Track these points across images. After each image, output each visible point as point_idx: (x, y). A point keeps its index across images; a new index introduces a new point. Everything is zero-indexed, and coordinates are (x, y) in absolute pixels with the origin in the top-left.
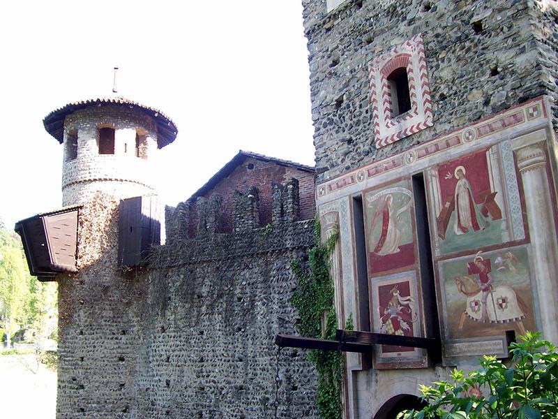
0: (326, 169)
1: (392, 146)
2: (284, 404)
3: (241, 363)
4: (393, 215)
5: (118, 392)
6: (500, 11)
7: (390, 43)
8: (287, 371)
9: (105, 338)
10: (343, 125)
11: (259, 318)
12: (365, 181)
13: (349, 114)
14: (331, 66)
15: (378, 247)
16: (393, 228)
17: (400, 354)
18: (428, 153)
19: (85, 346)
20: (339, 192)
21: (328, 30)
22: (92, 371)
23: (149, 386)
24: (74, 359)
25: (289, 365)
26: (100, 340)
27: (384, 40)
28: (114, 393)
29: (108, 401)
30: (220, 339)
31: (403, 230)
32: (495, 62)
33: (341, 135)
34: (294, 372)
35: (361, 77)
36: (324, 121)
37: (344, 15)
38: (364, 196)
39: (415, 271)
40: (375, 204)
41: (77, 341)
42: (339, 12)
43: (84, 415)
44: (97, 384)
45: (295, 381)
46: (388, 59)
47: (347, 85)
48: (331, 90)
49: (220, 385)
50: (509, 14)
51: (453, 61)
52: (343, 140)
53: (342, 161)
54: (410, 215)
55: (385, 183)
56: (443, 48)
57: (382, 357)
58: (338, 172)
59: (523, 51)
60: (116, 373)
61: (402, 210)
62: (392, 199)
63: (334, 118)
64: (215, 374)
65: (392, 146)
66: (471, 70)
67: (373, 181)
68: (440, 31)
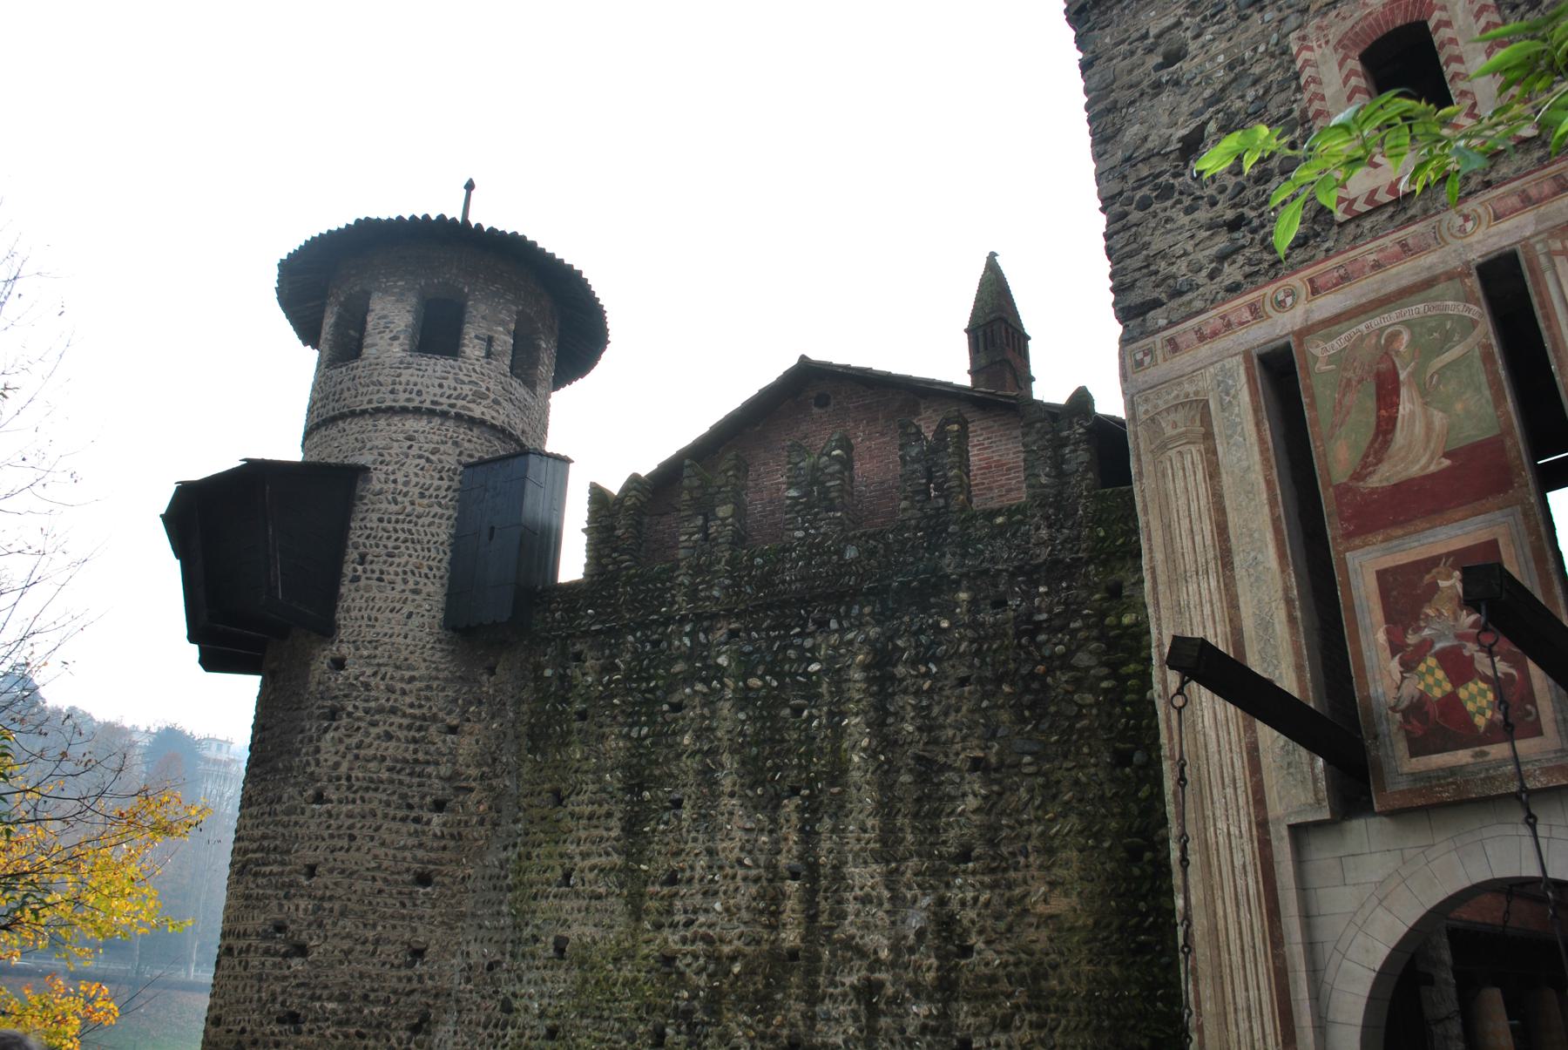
0: (1157, 304)
1: (1391, 209)
2: (930, 999)
3: (796, 885)
4: (1411, 374)
5: (404, 972)
8: (942, 902)
9: (385, 816)
11: (856, 759)
12: (1300, 310)
15: (1365, 466)
16: (1418, 410)
17: (1484, 754)
18: (1527, 201)
19: (326, 834)
20: (1205, 350)
22: (337, 906)
23: (498, 957)
24: (288, 868)
25: (948, 886)
26: (369, 821)
28: (394, 972)
29: (372, 996)
30: (736, 818)
31: (1459, 407)
33: (1203, 215)
34: (963, 903)
35: (1267, 72)
36: (1139, 195)
38: (1301, 344)
39: (1519, 508)
40: (1339, 359)
41: (302, 819)
43: (299, 1032)
44: (346, 944)
45: (967, 931)
48: (1165, 119)
49: (726, 949)
52: (1212, 226)
53: (1212, 276)
54: (1478, 364)
55: (1371, 302)
57: (1406, 769)
58: (1198, 304)
60: (403, 917)
61: (1447, 357)
62: (1405, 337)
63: (1176, 182)
64: (712, 917)
65: (1391, 209)
67: (1329, 304)
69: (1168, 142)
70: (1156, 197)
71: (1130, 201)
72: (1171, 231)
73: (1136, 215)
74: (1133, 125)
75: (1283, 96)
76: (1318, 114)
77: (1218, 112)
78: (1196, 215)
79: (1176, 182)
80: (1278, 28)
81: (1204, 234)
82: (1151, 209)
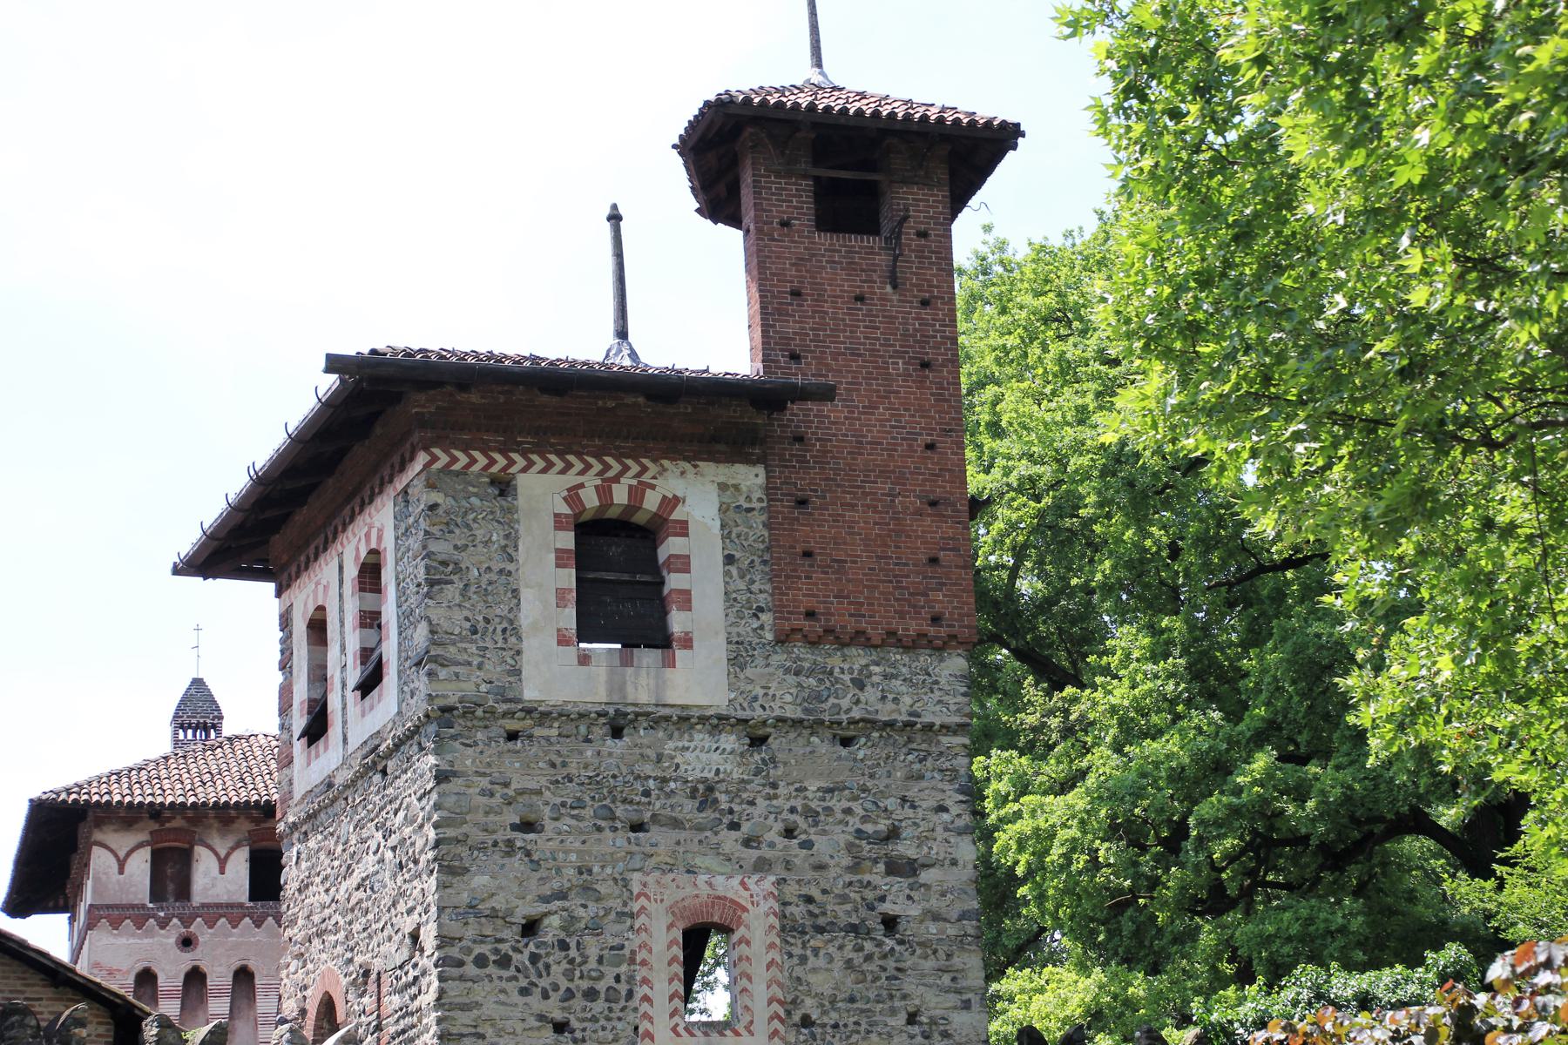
6: (936, 917)
7: (693, 858)
10: (544, 982)
13: (565, 965)
14: (514, 827)
21: (512, 736)
27: (678, 843)
32: (917, 1002)
33: (535, 1001)
36: (478, 950)
37: (569, 728)
42: (561, 715)
46: (690, 891)
47: (562, 895)
48: (515, 889)
50: (952, 931)
51: (838, 964)
52: (541, 1017)
56: (821, 930)
59: (967, 1005)
66: (872, 995)
68: (816, 893)
69: (510, 912)
70: (494, 962)
71: (469, 951)
72: (503, 1004)
73: (471, 970)
74: (483, 874)
75: (617, 928)
76: (644, 963)
77: (564, 909)
78: (528, 999)
79: (516, 957)
80: (623, 859)
81: (534, 1023)
82: (488, 971)
